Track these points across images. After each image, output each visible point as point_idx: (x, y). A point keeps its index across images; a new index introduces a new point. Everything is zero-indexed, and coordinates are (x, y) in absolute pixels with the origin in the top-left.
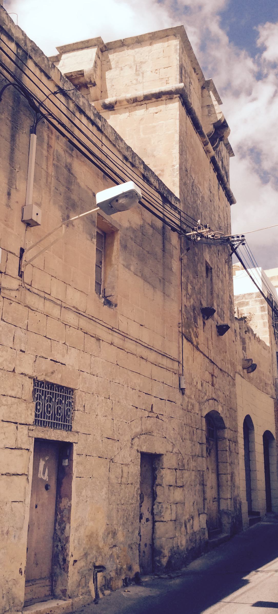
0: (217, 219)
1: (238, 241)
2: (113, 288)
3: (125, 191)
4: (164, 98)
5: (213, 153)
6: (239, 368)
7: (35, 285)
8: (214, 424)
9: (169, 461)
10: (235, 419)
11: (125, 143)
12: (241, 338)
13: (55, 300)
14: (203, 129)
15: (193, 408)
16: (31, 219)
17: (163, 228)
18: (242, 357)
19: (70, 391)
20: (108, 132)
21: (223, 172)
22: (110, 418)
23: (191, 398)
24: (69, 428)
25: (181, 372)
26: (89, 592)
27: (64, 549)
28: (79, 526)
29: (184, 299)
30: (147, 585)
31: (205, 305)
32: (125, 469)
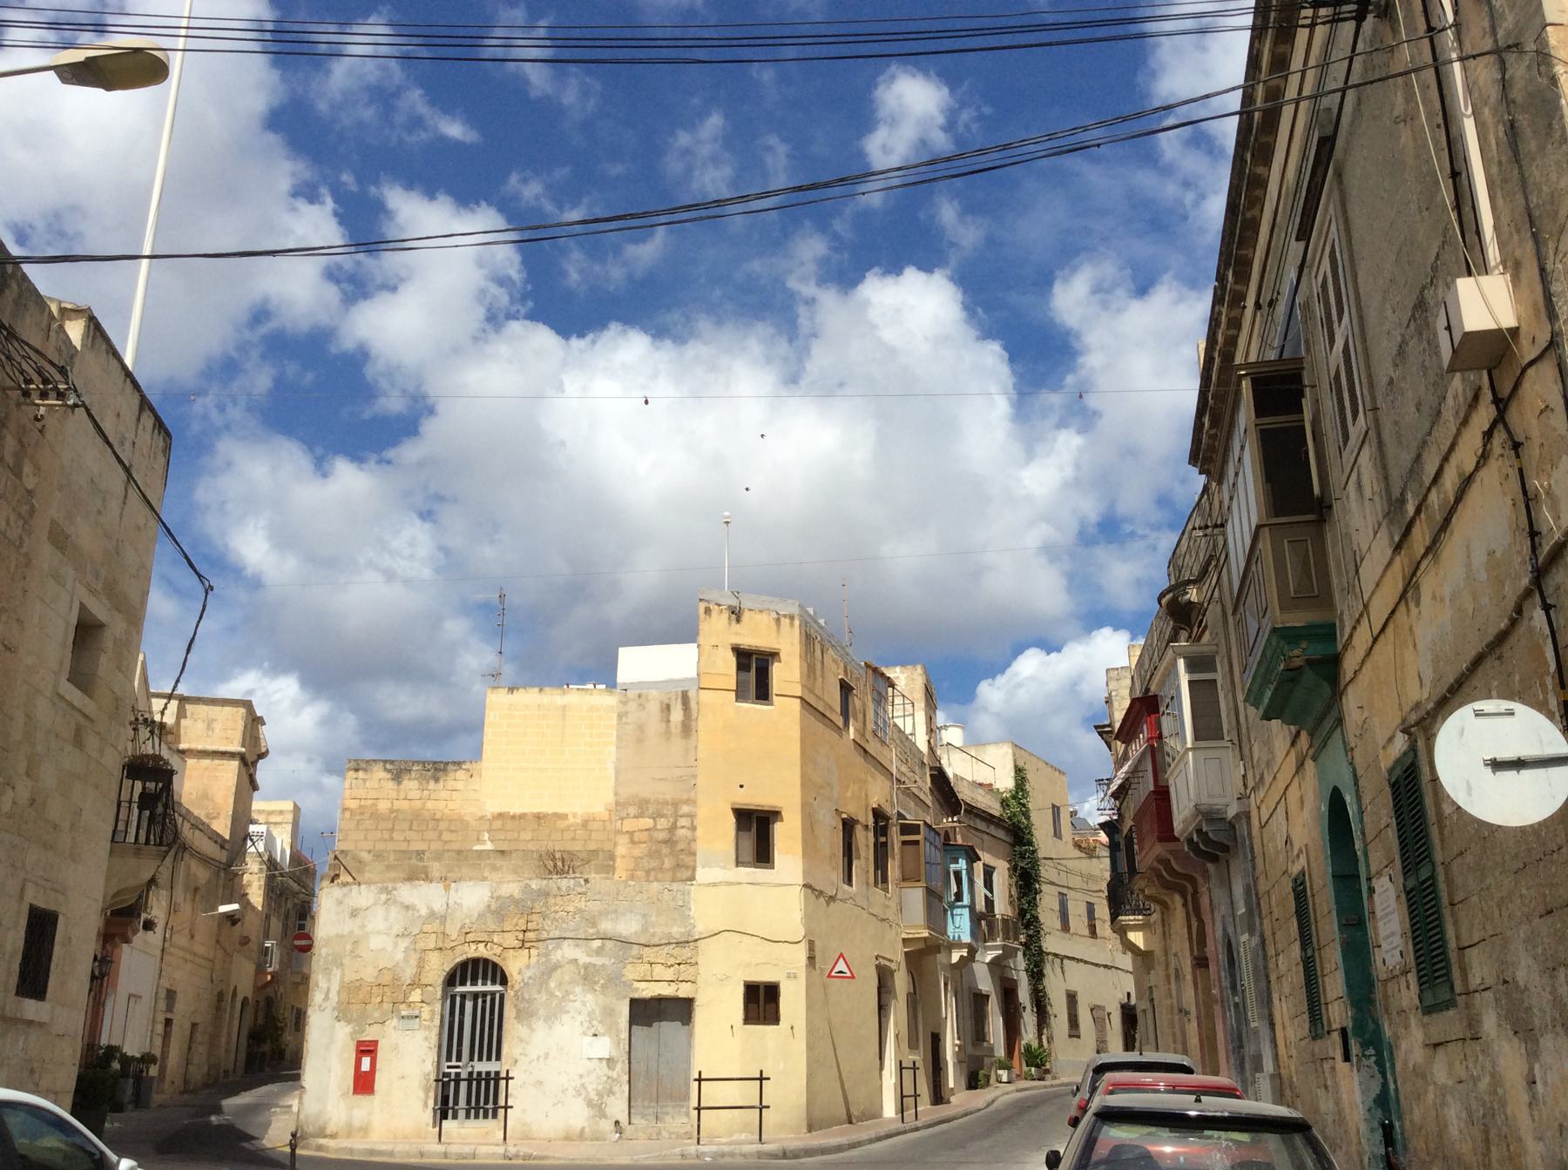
8: (221, 996)
9: (200, 1028)
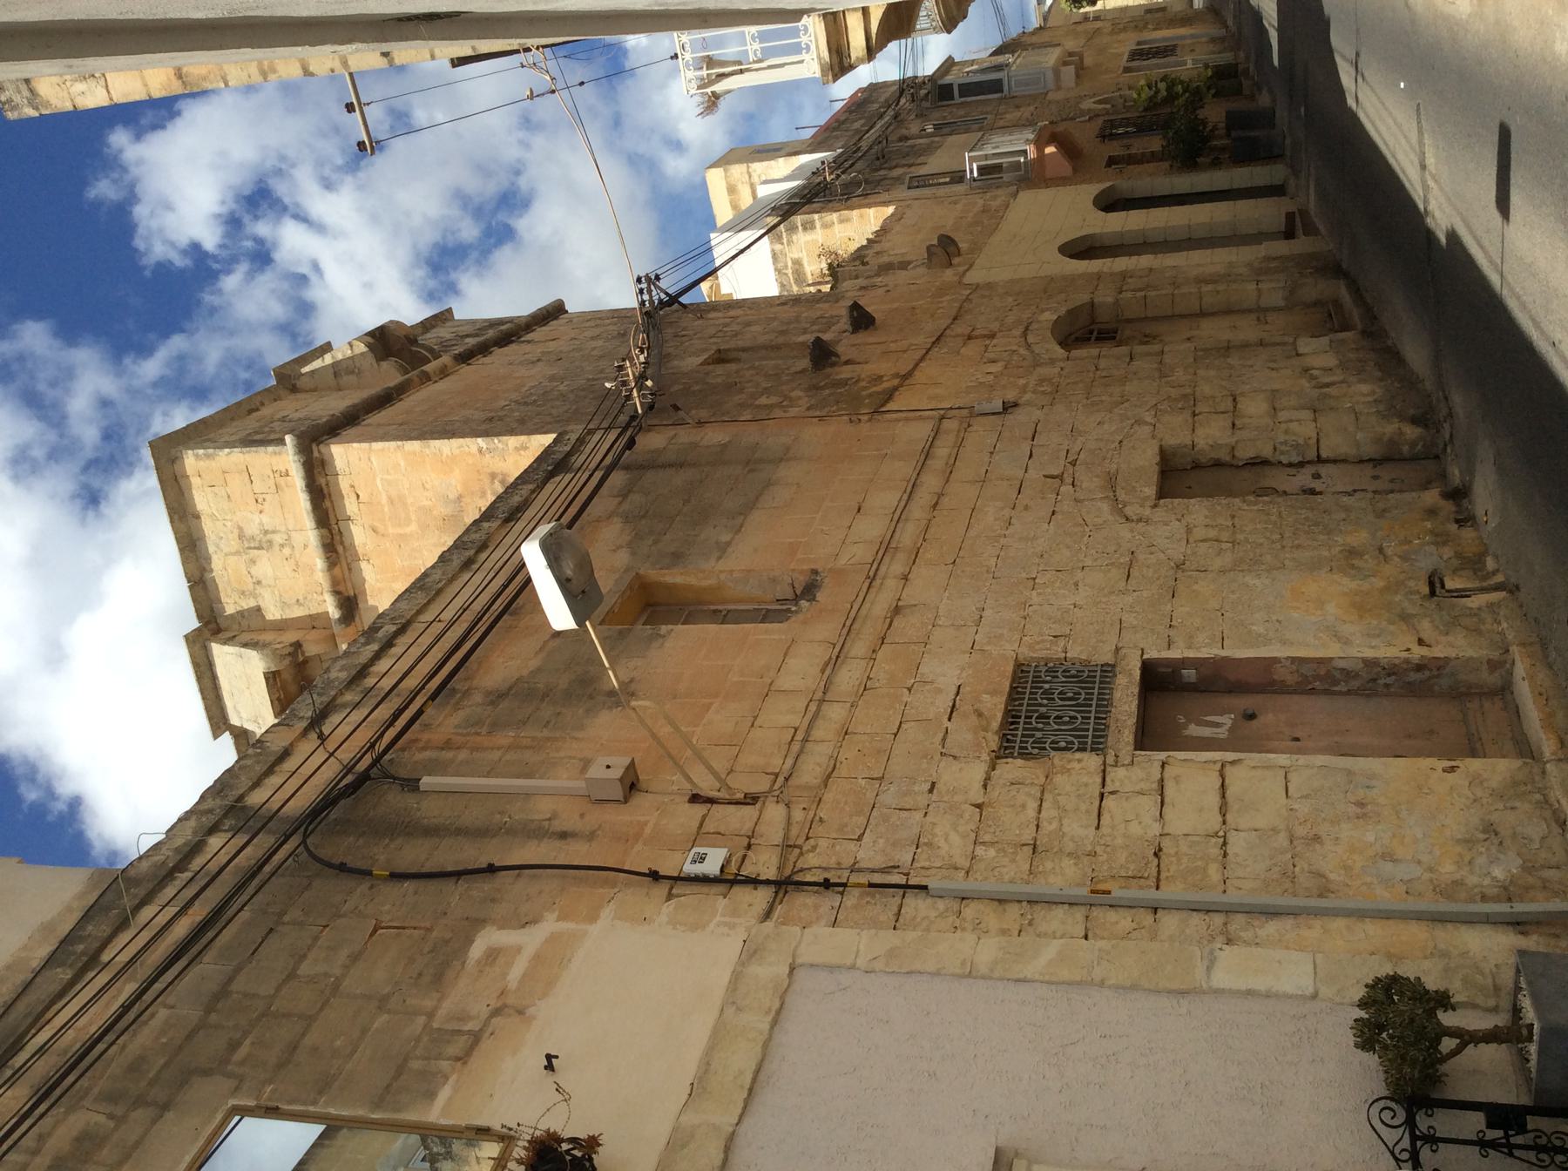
0: (600, 343)
1: (650, 292)
2: (774, 580)
3: (544, 562)
4: (322, 481)
5: (446, 359)
6: (949, 275)
7: (776, 763)
9: (1176, 432)
10: (1070, 281)
11: (433, 567)
12: (878, 275)
13: (809, 715)
14: (392, 384)
15: (1050, 380)
16: (621, 780)
17: (627, 468)
18: (922, 270)
19: (1020, 669)
20: (407, 609)
21: (491, 333)
22: (1079, 575)
23: (1026, 386)
24: (1109, 670)
25: (965, 412)
26: (1490, 606)
27: (1392, 670)
28: (1337, 637)
29: (793, 411)
30: (1470, 470)
31: (805, 363)
32: (1199, 533)
